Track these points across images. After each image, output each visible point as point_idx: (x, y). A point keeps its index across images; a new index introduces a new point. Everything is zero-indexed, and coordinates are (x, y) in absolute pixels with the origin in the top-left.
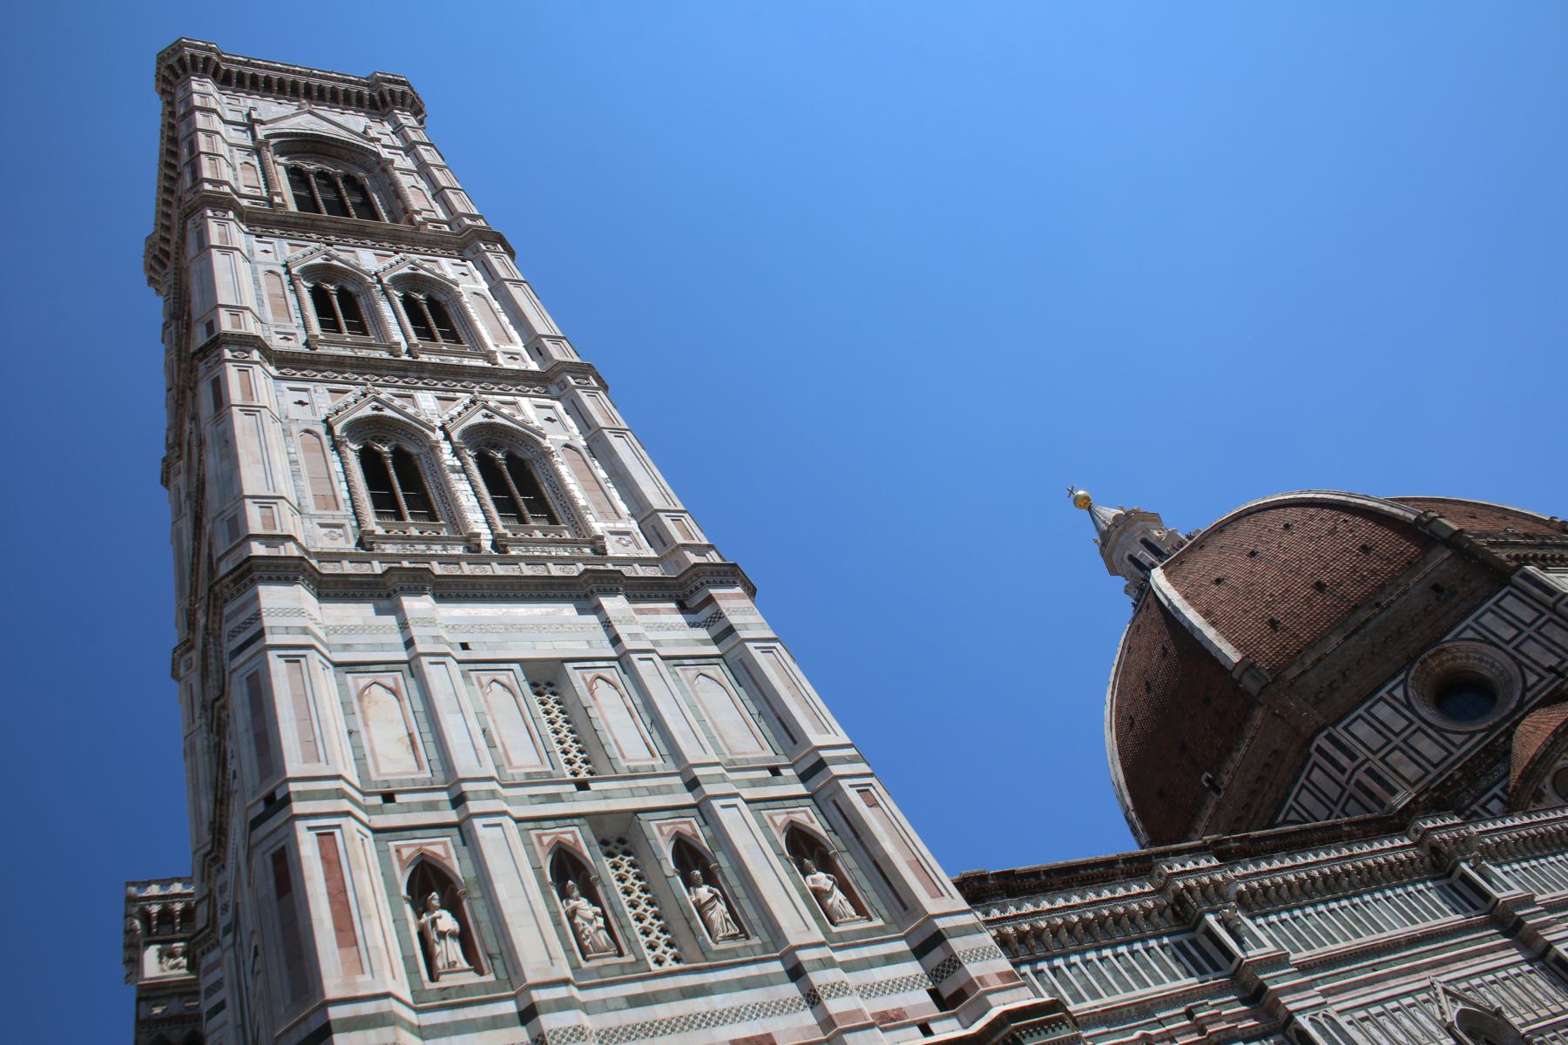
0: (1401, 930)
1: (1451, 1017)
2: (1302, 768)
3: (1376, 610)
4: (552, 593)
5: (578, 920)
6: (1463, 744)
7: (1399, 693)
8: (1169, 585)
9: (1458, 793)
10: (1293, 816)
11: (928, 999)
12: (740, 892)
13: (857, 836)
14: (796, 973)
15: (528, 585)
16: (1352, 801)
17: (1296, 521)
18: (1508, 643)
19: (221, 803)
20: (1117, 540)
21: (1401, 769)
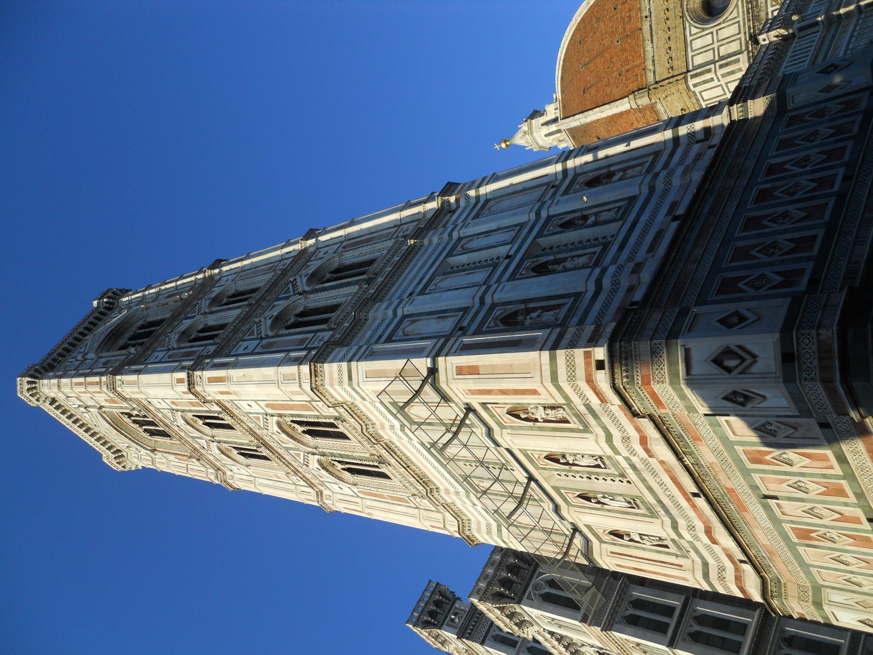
2: (698, 100)
3: (648, 19)
4: (410, 258)
6: (738, 13)
7: (694, 31)
15: (400, 265)
19: (409, 467)
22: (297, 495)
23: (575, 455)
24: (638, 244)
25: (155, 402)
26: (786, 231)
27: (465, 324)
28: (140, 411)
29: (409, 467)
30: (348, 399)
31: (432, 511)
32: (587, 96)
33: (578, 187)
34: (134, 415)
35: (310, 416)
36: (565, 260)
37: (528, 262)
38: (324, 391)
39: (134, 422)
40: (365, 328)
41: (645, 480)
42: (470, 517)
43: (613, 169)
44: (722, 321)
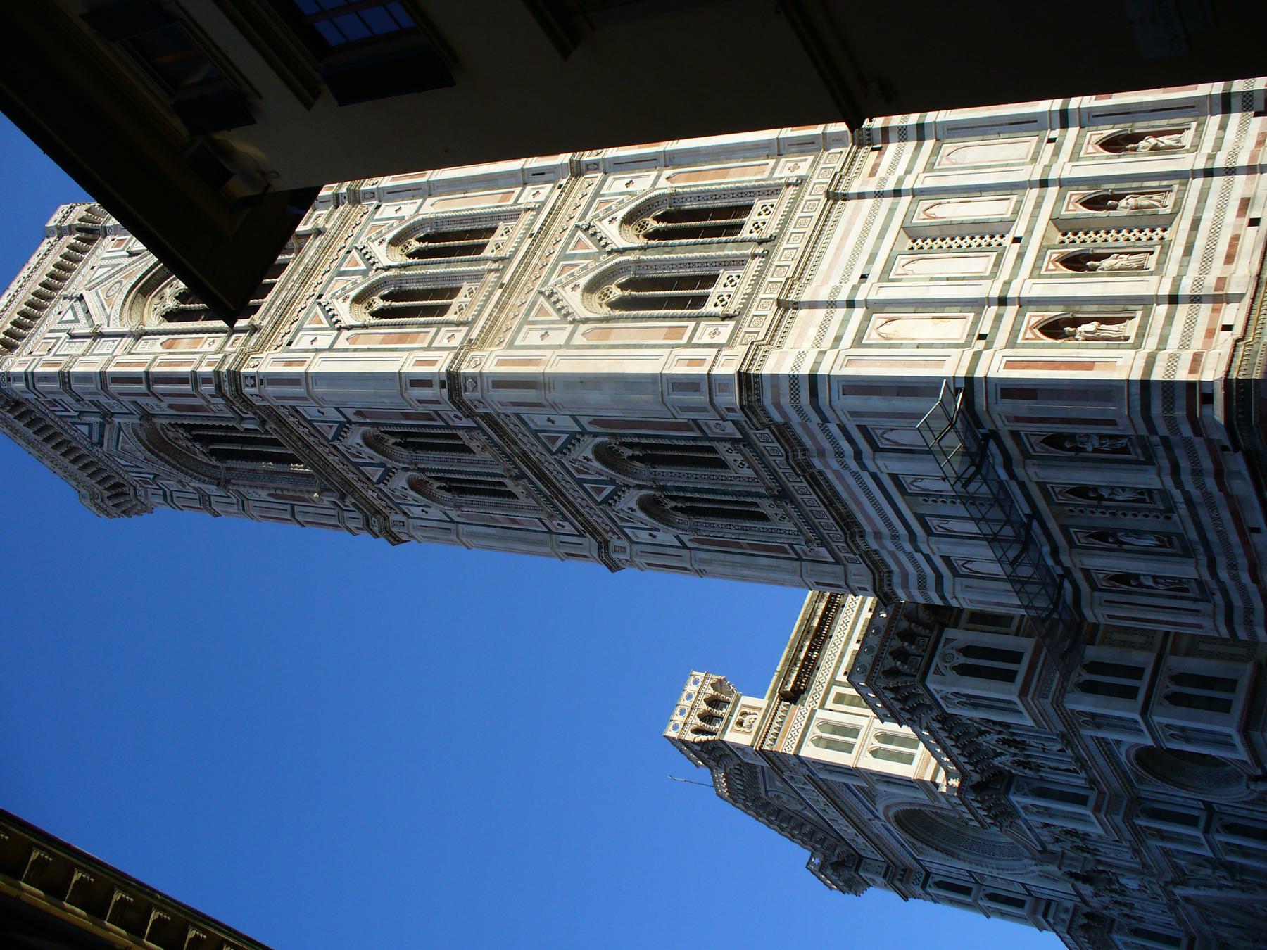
11: (1260, 119)
12: (1135, 185)
13: (1128, 113)
14: (1209, 173)
19: (831, 504)
22: (552, 548)
23: (1112, 488)
25: (311, 412)
27: (985, 329)
28: (263, 423)
30: (795, 419)
31: (825, 562)
33: (1091, 149)
34: (242, 430)
35: (678, 438)
36: (1107, 256)
37: (1052, 253)
38: (758, 410)
39: (197, 439)
41: (1197, 515)
42: (894, 567)
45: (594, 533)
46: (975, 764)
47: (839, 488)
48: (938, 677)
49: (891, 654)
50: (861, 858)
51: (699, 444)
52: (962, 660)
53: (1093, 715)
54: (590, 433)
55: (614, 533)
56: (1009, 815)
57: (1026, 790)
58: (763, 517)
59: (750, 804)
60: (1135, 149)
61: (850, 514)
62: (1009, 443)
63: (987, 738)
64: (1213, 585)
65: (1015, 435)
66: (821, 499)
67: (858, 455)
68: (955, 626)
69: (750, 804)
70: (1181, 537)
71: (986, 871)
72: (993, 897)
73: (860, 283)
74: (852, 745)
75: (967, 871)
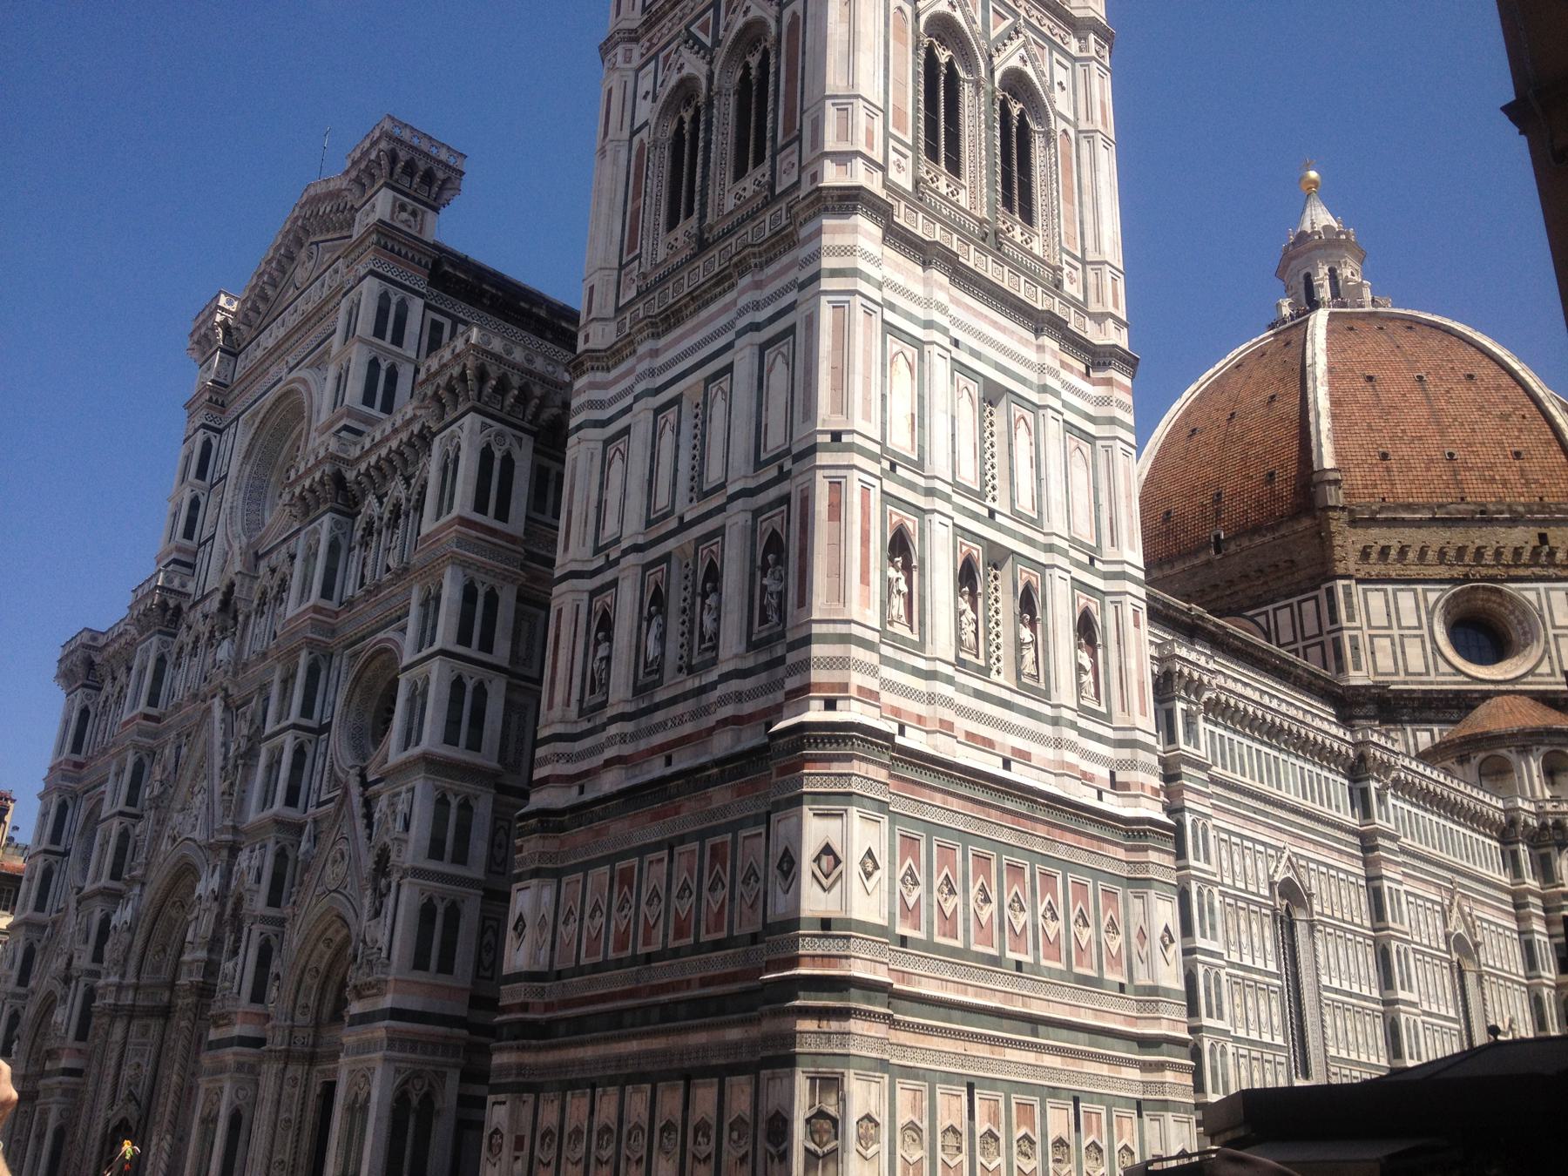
0: (1293, 798)
1: (1278, 878)
2: (1303, 593)
5: (963, 618)
6: (1444, 674)
7: (1432, 597)
8: (1324, 347)
9: (1405, 706)
10: (1262, 620)
13: (1119, 643)
16: (1318, 648)
17: (1482, 380)
18: (1554, 627)
19: (692, 299)
20: (1310, 250)
21: (1379, 656)
23: (718, 609)
24: (980, 718)
26: (966, 905)
27: (900, 471)
29: (692, 299)
32: (1361, 383)
33: (1082, 602)
36: (974, 608)
40: (909, 264)
41: (685, 699)
42: (614, 373)
43: (1100, 652)
44: (870, 853)
45: (649, 24)
46: (367, 474)
47: (713, 308)
48: (478, 426)
49: (505, 375)
50: (236, 355)
51: (768, 144)
52: (498, 455)
53: (438, 598)
54: (781, 13)
55: (649, 49)
56: (306, 514)
57: (337, 531)
58: (672, 224)
59: (300, 223)
60: (1080, 646)
61: (678, 323)
62: (773, 493)
63: (401, 486)
64: (600, 719)
65: (785, 499)
66: (699, 287)
67: (755, 327)
68: (536, 451)
69: (300, 223)
70: (659, 683)
71: (228, 495)
72: (195, 504)
73: (950, 337)
74: (383, 338)
75: (226, 476)
